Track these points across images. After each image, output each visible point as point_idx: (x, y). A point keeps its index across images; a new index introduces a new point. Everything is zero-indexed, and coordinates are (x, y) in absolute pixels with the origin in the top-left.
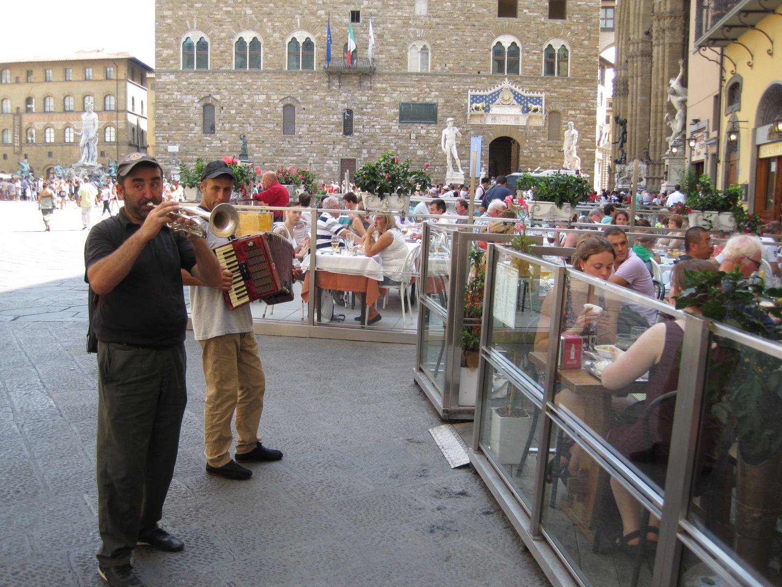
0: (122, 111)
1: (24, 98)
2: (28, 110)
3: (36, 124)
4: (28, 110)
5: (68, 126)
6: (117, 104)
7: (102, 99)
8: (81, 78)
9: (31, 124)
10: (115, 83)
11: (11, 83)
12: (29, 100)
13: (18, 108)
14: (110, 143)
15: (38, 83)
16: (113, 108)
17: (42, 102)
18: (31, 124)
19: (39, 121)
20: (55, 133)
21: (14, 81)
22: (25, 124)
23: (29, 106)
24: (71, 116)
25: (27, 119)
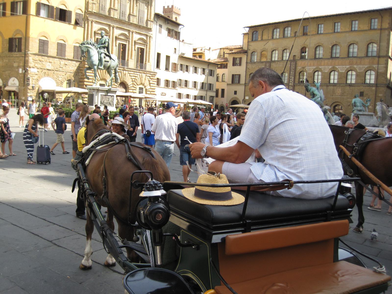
0: (383, 57)
1: (300, 48)
2: (302, 58)
3: (307, 68)
4: (302, 58)
5: (333, 70)
6: (379, 50)
7: (366, 47)
8: (347, 30)
9: (304, 68)
10: (379, 32)
11: (291, 37)
12: (303, 50)
13: (294, 56)
14: (370, 85)
15: (312, 35)
16: (375, 54)
17: (314, 50)
18: (304, 68)
19: (310, 66)
20: (322, 75)
21: (293, 35)
22: (299, 68)
23: (303, 54)
24: (337, 61)
25: (300, 64)
